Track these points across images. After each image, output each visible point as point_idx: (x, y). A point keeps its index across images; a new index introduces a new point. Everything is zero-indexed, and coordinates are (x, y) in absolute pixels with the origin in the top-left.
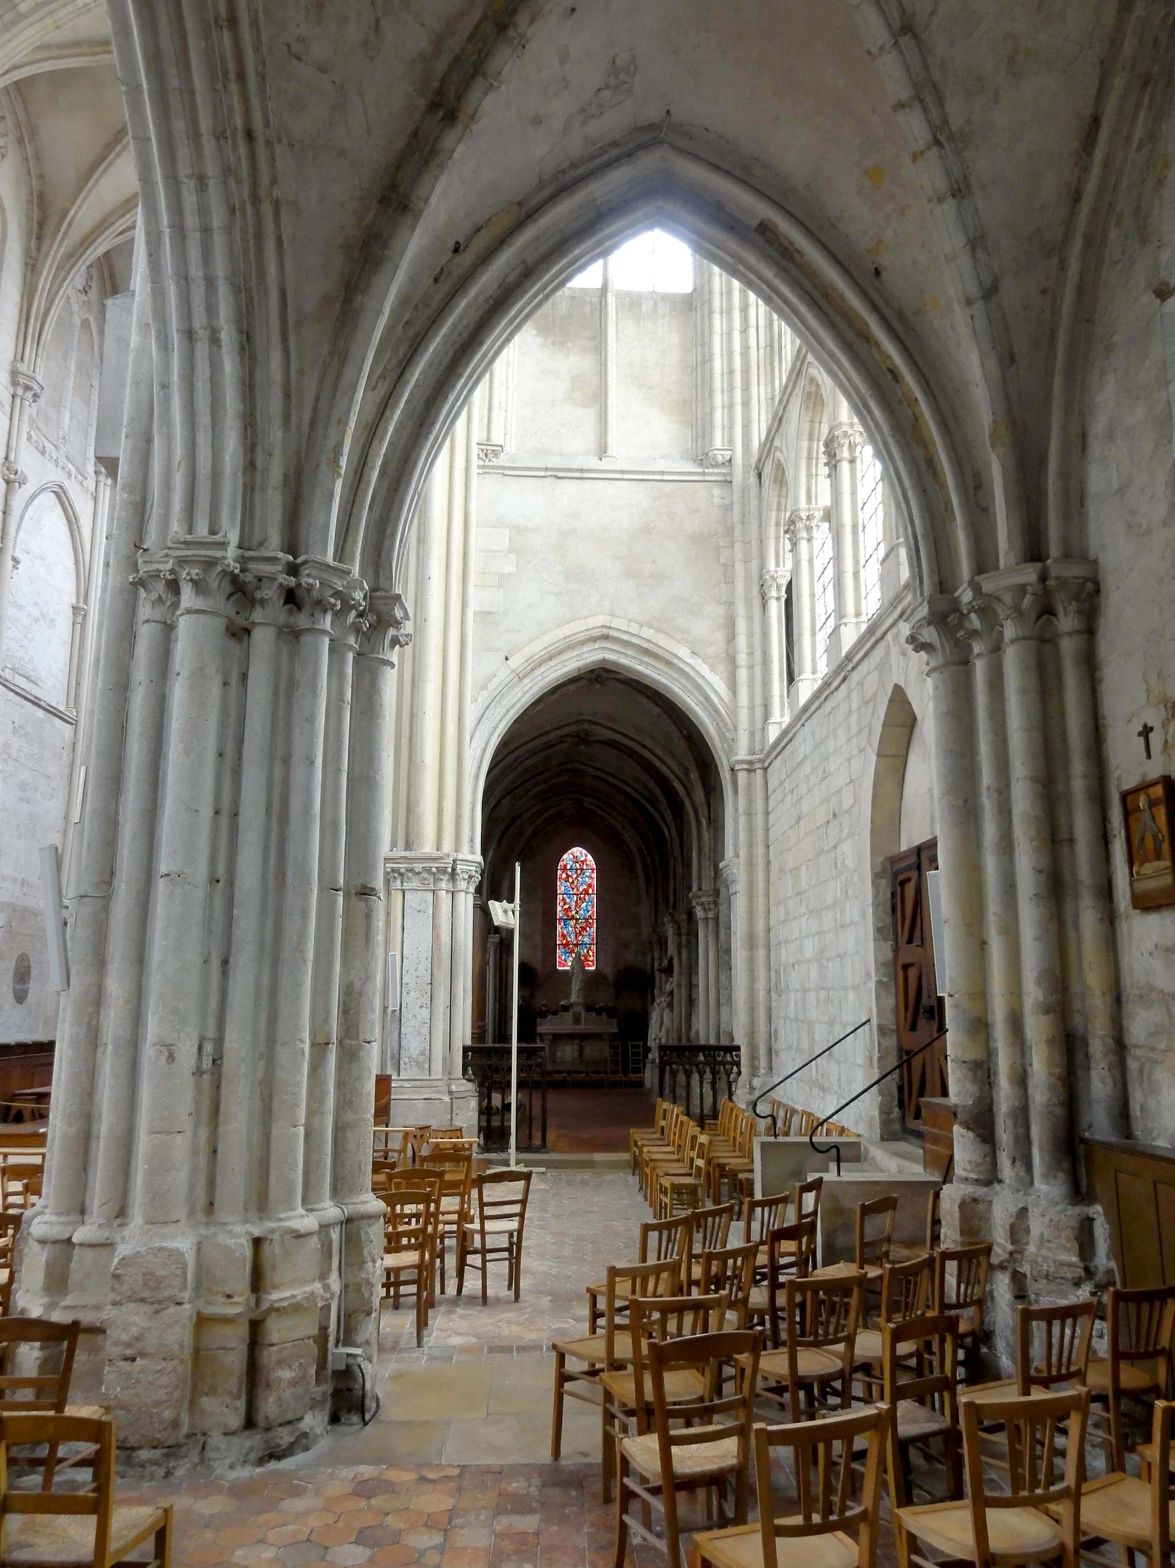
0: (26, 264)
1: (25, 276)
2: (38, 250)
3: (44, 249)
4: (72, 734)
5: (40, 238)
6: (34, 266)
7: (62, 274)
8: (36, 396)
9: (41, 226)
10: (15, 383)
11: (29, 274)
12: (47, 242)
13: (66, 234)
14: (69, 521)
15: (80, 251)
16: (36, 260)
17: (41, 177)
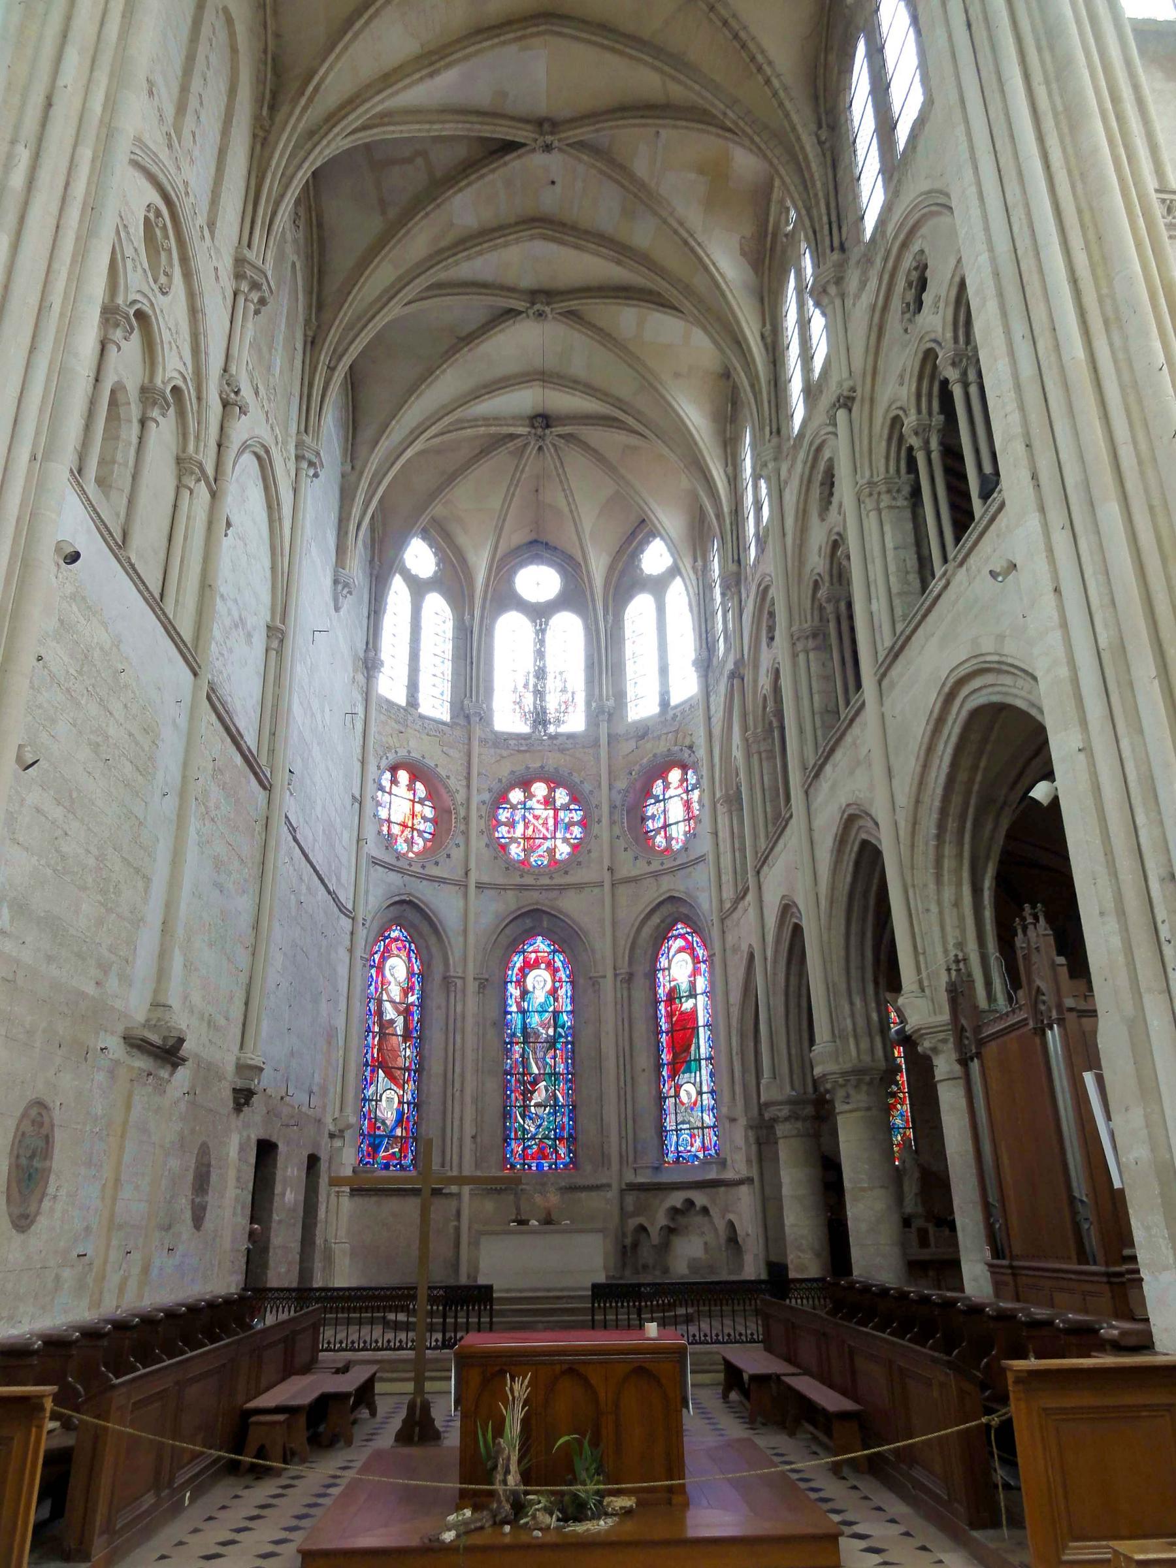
0: (255, 136)
1: (253, 149)
2: (272, 118)
3: (280, 117)
4: (266, 801)
5: (273, 108)
6: (265, 139)
7: (302, 154)
8: (262, 302)
9: (274, 95)
10: (238, 276)
11: (258, 147)
12: (285, 109)
13: (311, 100)
14: (270, 507)
15: (325, 128)
16: (268, 132)
17: (277, 36)
